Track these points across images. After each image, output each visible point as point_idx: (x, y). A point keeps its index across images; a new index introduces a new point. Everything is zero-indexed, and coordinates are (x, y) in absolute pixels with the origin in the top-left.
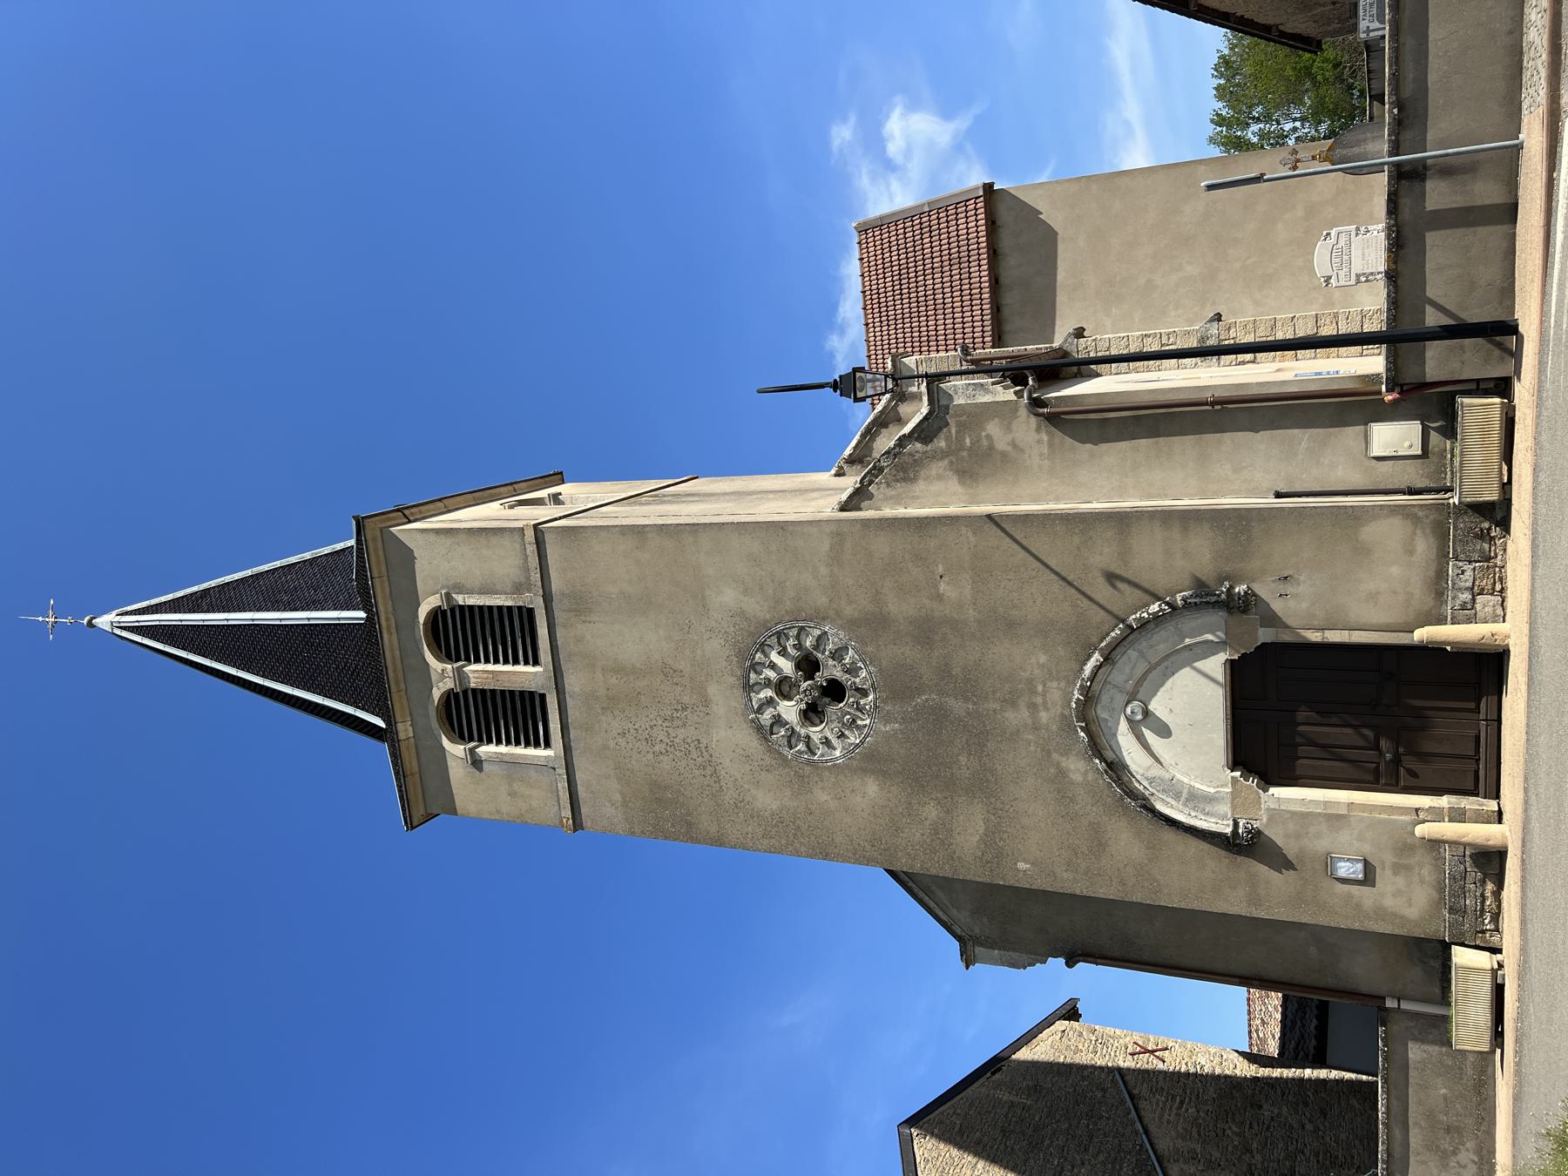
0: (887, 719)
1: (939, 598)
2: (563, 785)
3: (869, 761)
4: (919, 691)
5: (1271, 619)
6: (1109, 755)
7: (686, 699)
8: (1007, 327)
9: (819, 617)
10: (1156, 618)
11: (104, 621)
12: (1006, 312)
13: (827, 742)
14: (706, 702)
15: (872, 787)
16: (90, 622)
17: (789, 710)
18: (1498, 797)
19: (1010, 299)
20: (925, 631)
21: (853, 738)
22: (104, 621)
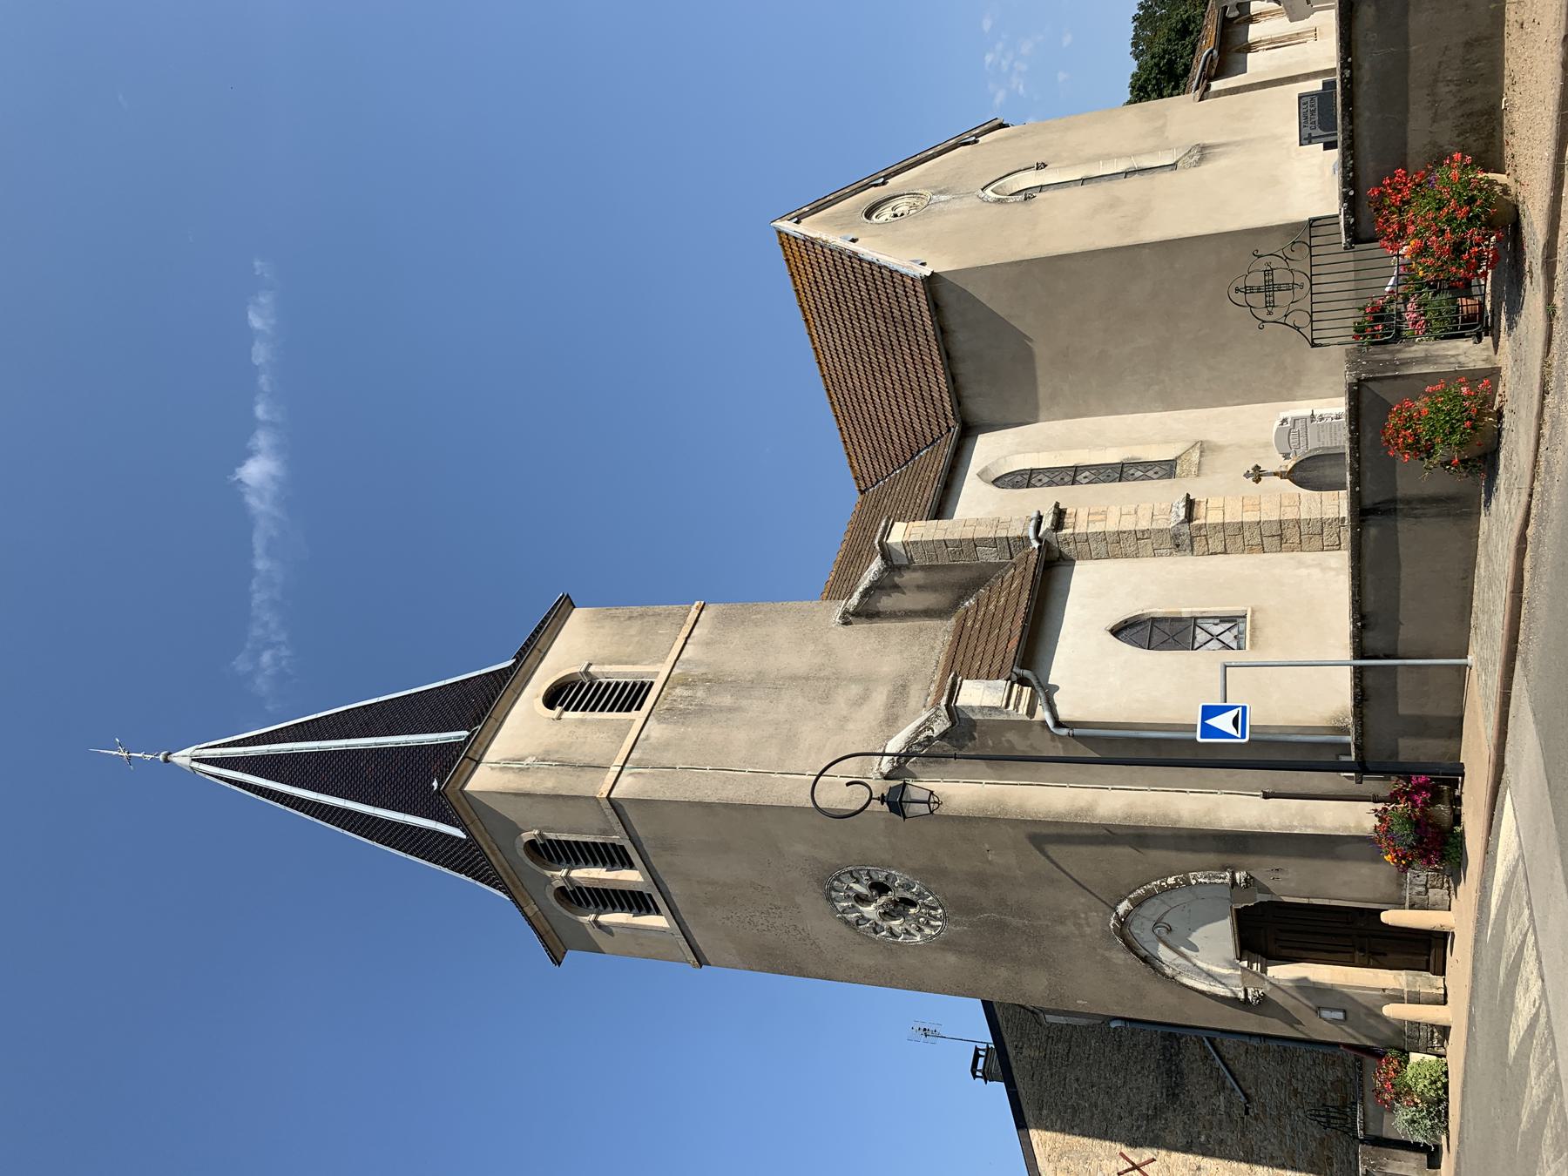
0: (956, 924)
1: (990, 863)
2: (683, 943)
3: (947, 944)
4: (982, 910)
5: (1267, 891)
6: (1143, 953)
7: (778, 903)
8: (965, 393)
9: (884, 865)
10: (1172, 887)
11: (182, 758)
12: (961, 380)
13: (908, 932)
14: (798, 906)
15: (952, 958)
16: (166, 761)
17: (870, 911)
18: (1444, 973)
19: (965, 369)
20: (981, 880)
21: (927, 931)
22: (182, 758)
